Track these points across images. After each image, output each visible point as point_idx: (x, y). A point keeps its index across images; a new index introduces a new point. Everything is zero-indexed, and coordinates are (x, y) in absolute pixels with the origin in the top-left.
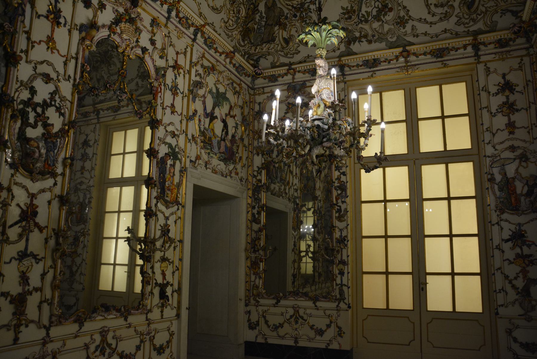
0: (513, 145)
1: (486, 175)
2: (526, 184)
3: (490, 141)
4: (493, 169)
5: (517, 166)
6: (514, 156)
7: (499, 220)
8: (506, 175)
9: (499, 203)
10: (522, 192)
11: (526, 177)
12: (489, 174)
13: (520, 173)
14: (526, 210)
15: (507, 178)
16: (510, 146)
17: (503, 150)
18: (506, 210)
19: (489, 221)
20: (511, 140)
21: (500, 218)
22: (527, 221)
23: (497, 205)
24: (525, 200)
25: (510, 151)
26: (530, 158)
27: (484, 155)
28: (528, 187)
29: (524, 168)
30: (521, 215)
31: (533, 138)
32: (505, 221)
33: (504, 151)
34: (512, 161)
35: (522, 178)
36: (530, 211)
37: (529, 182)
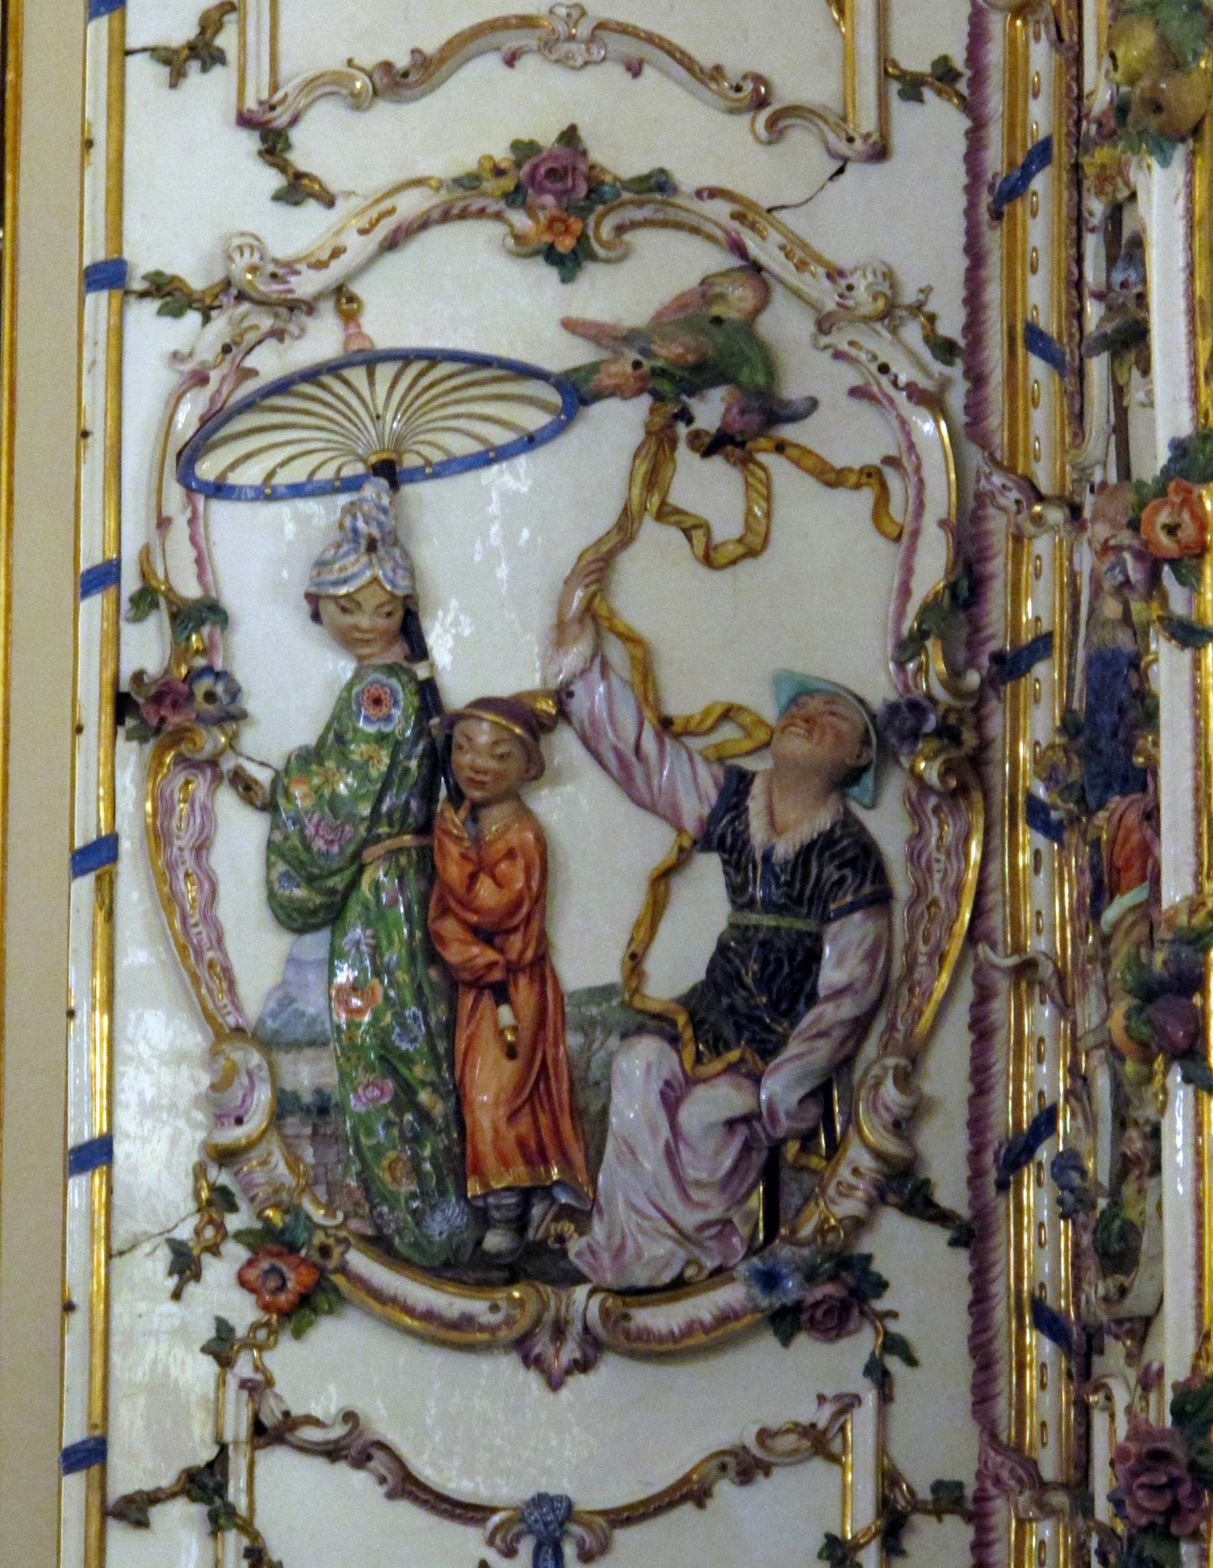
0: (570, 136)
1: (93, 608)
2: (707, 840)
3: (210, 24)
4: (221, 513)
5: (604, 520)
6: (570, 326)
7: (237, 1426)
8: (418, 650)
9: (256, 1122)
10: (635, 961)
11: (728, 713)
12: (146, 600)
13: (630, 639)
14: (679, 1287)
15: (428, 692)
16: (524, 150)
17: (410, 204)
18: (360, 1261)
19: (75, 1432)
20: (547, 46)
21: (257, 1388)
22: (663, 1477)
23: (226, 1156)
24: (672, 1098)
25: (522, 248)
26: (813, 404)
27: (95, 251)
28: (736, 891)
29: (708, 560)
30: (583, 1366)
31: (887, 69)
32: (332, 1452)
33: (423, 224)
34: (535, 419)
35: (666, 723)
36: (731, 1295)
37: (755, 805)
